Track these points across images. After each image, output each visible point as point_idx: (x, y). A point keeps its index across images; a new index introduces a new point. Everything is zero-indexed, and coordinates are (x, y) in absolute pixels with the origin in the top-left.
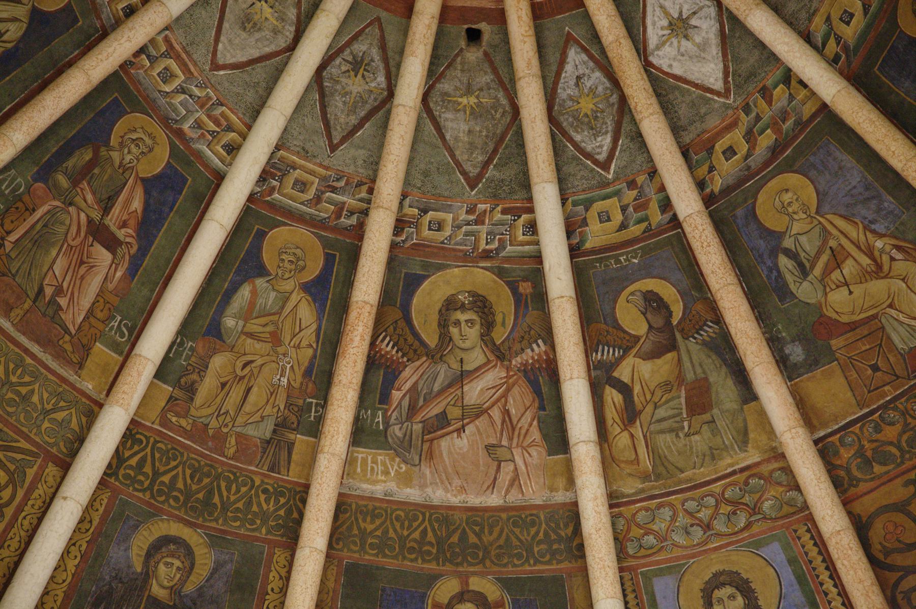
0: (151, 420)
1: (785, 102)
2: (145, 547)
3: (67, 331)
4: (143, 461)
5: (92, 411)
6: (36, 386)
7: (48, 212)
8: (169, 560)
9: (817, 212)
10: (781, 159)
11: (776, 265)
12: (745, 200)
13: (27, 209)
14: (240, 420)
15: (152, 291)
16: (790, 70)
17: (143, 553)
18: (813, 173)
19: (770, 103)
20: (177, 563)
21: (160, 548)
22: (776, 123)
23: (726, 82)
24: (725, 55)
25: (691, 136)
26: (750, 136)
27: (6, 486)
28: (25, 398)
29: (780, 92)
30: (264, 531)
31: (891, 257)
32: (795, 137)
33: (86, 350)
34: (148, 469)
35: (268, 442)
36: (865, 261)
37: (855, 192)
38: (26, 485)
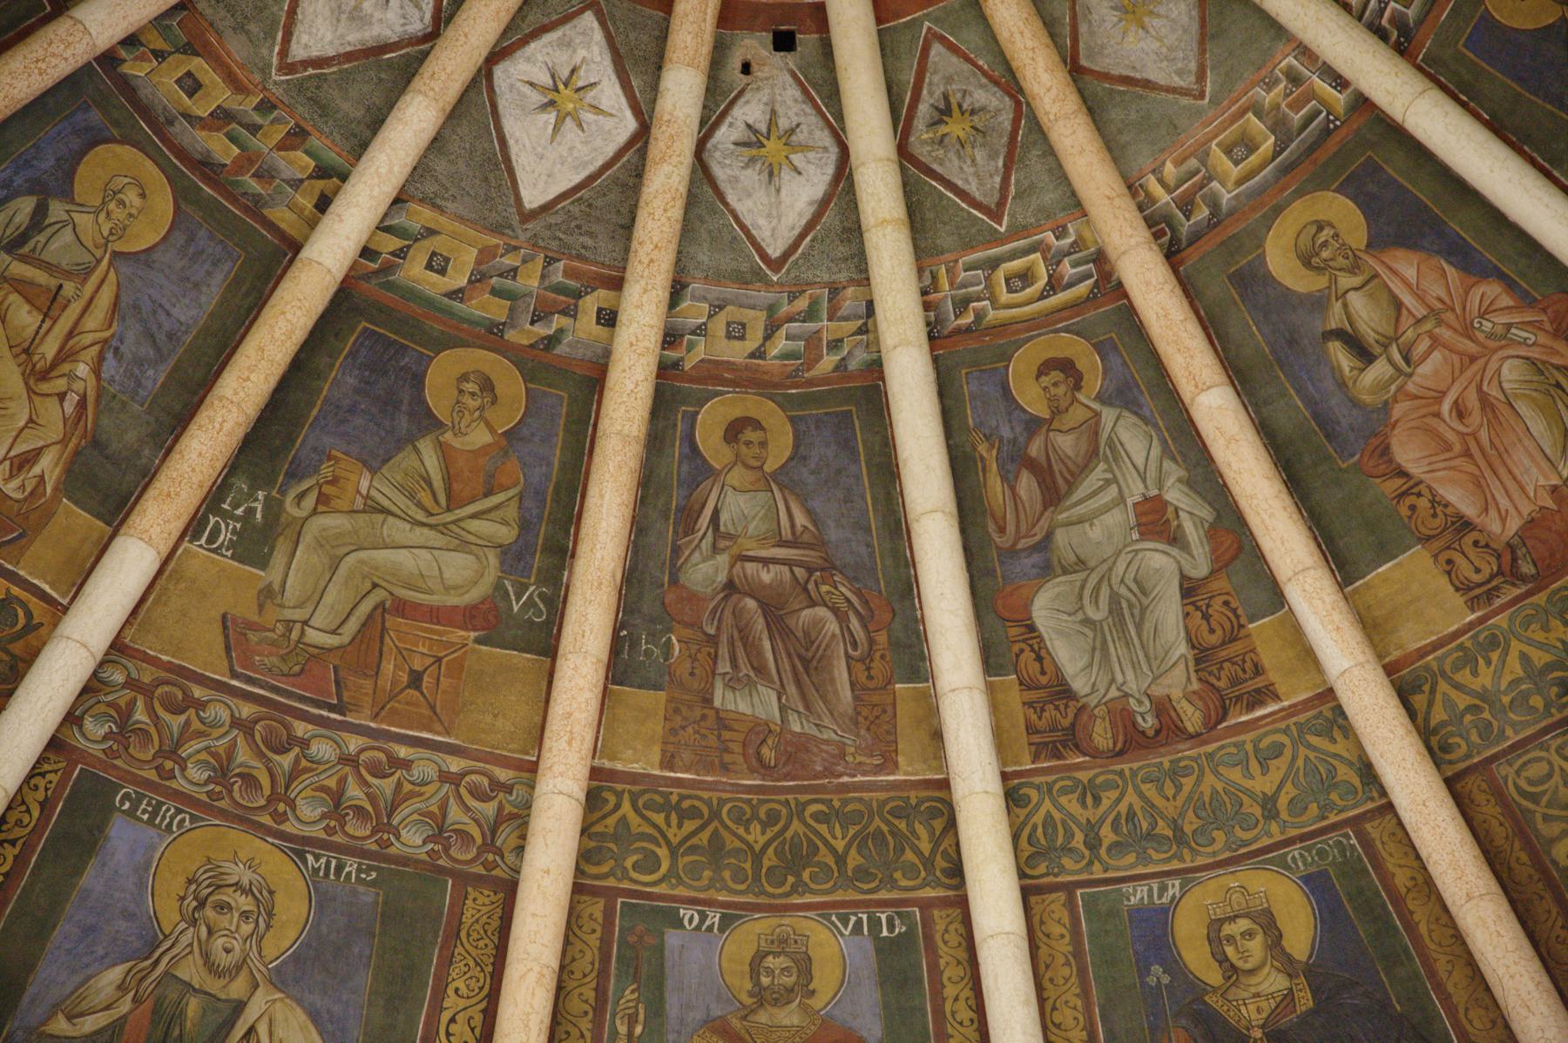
1: (287, 174)
9: (116, 255)
10: (195, 178)
11: (16, 194)
12: (116, 123)
16: (344, 177)
18: (180, 238)
19: (282, 146)
22: (251, 162)
23: (306, 63)
24: (349, 56)
25: (208, 12)
26: (223, 117)
29: (299, 163)
31: (65, 394)
32: (233, 199)
36: (49, 349)
37: (162, 317)
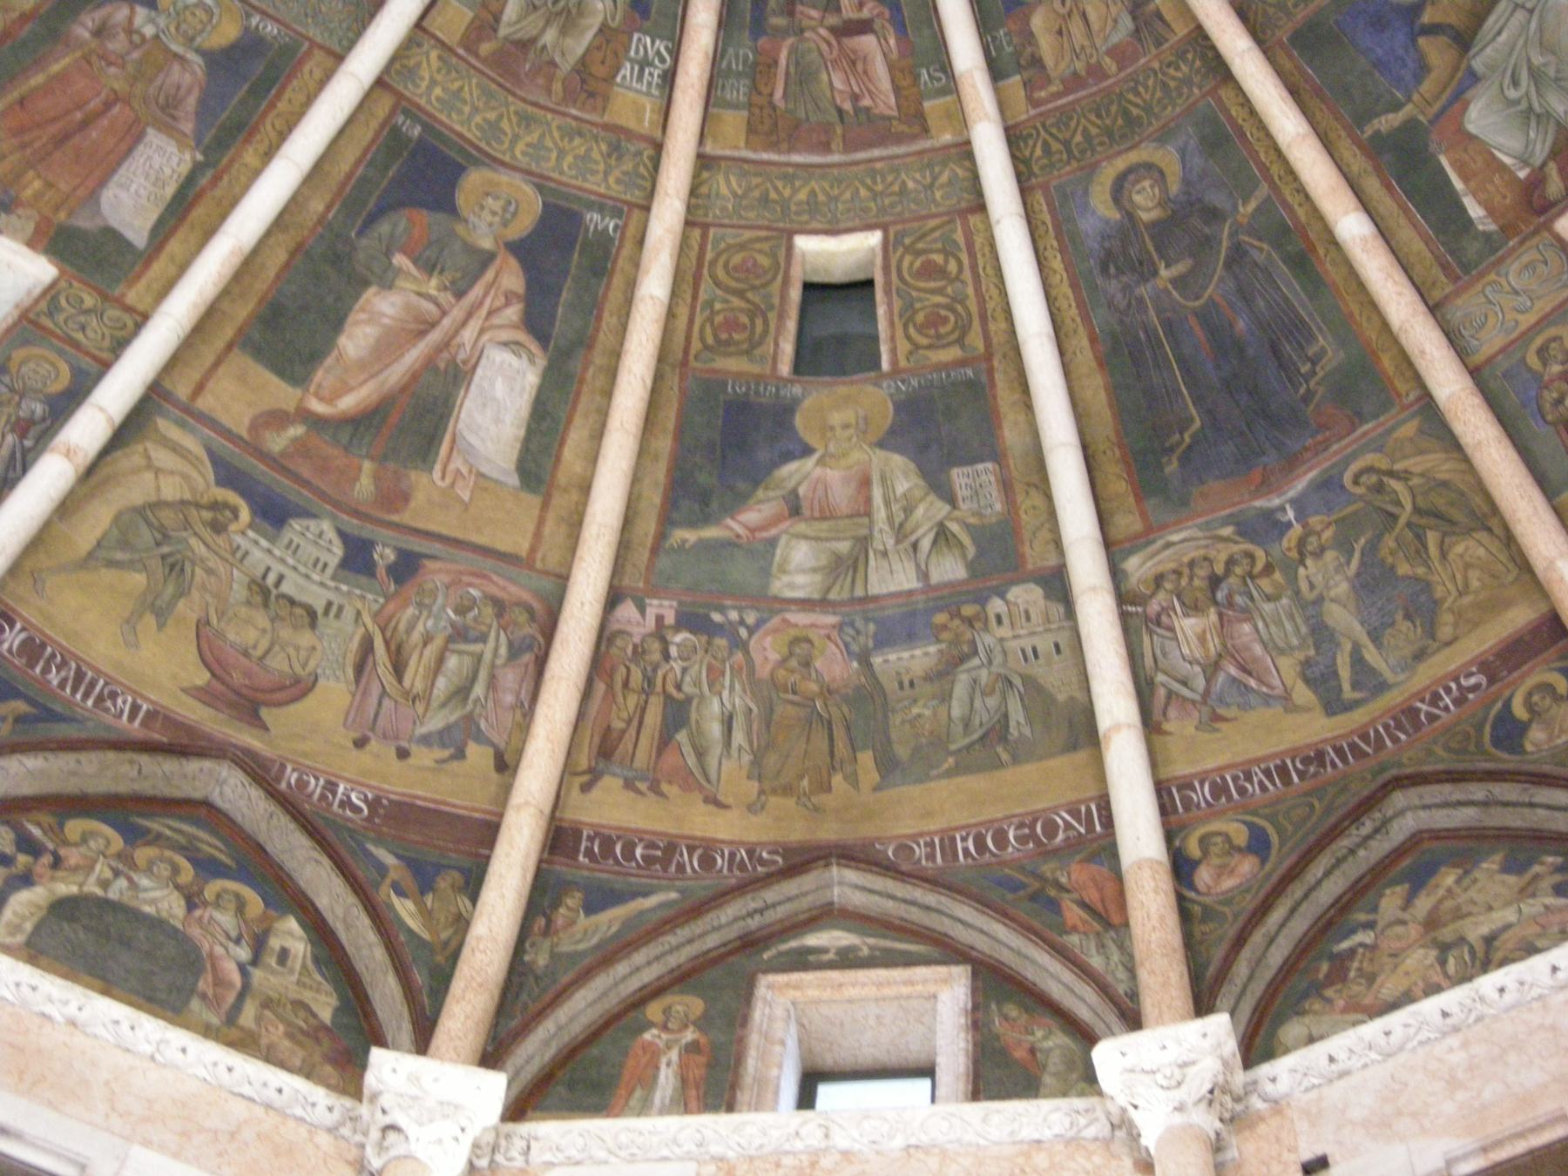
0: (1022, 112)
2: (1108, 197)
3: (890, 118)
4: (1045, 143)
5: (965, 152)
6: (903, 176)
7: (790, 54)
8: (1138, 187)
13: (769, 66)
14: (1098, 42)
15: (931, 26)
17: (1111, 203)
20: (1147, 183)
21: (1122, 187)
27: (946, 262)
28: (903, 190)
30: (1196, 91)
33: (920, 116)
34: (1055, 146)
35: (1137, 30)
38: (963, 246)
